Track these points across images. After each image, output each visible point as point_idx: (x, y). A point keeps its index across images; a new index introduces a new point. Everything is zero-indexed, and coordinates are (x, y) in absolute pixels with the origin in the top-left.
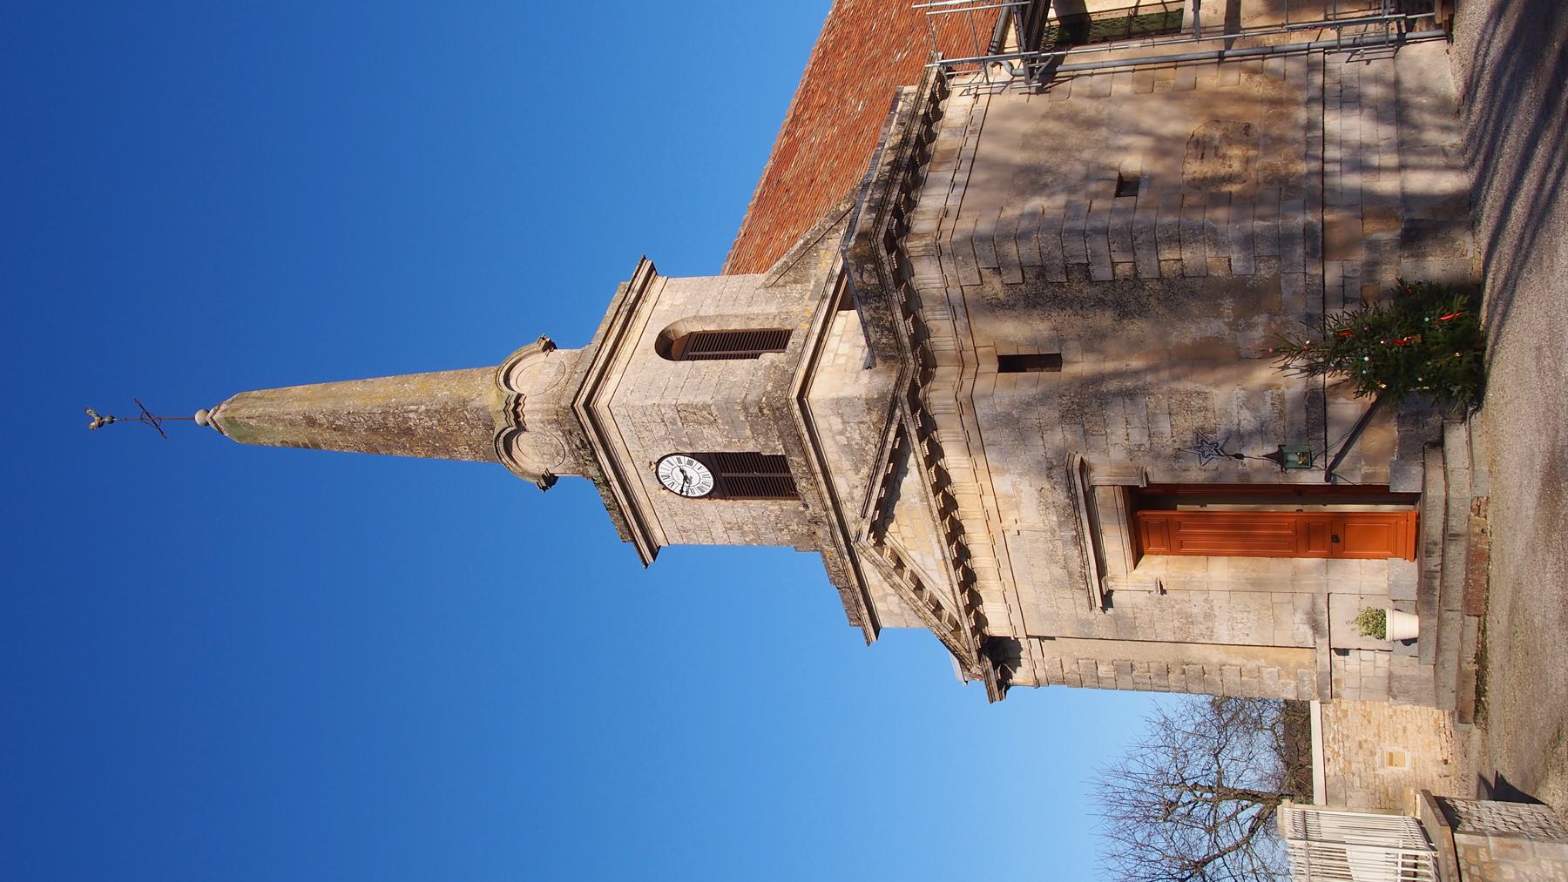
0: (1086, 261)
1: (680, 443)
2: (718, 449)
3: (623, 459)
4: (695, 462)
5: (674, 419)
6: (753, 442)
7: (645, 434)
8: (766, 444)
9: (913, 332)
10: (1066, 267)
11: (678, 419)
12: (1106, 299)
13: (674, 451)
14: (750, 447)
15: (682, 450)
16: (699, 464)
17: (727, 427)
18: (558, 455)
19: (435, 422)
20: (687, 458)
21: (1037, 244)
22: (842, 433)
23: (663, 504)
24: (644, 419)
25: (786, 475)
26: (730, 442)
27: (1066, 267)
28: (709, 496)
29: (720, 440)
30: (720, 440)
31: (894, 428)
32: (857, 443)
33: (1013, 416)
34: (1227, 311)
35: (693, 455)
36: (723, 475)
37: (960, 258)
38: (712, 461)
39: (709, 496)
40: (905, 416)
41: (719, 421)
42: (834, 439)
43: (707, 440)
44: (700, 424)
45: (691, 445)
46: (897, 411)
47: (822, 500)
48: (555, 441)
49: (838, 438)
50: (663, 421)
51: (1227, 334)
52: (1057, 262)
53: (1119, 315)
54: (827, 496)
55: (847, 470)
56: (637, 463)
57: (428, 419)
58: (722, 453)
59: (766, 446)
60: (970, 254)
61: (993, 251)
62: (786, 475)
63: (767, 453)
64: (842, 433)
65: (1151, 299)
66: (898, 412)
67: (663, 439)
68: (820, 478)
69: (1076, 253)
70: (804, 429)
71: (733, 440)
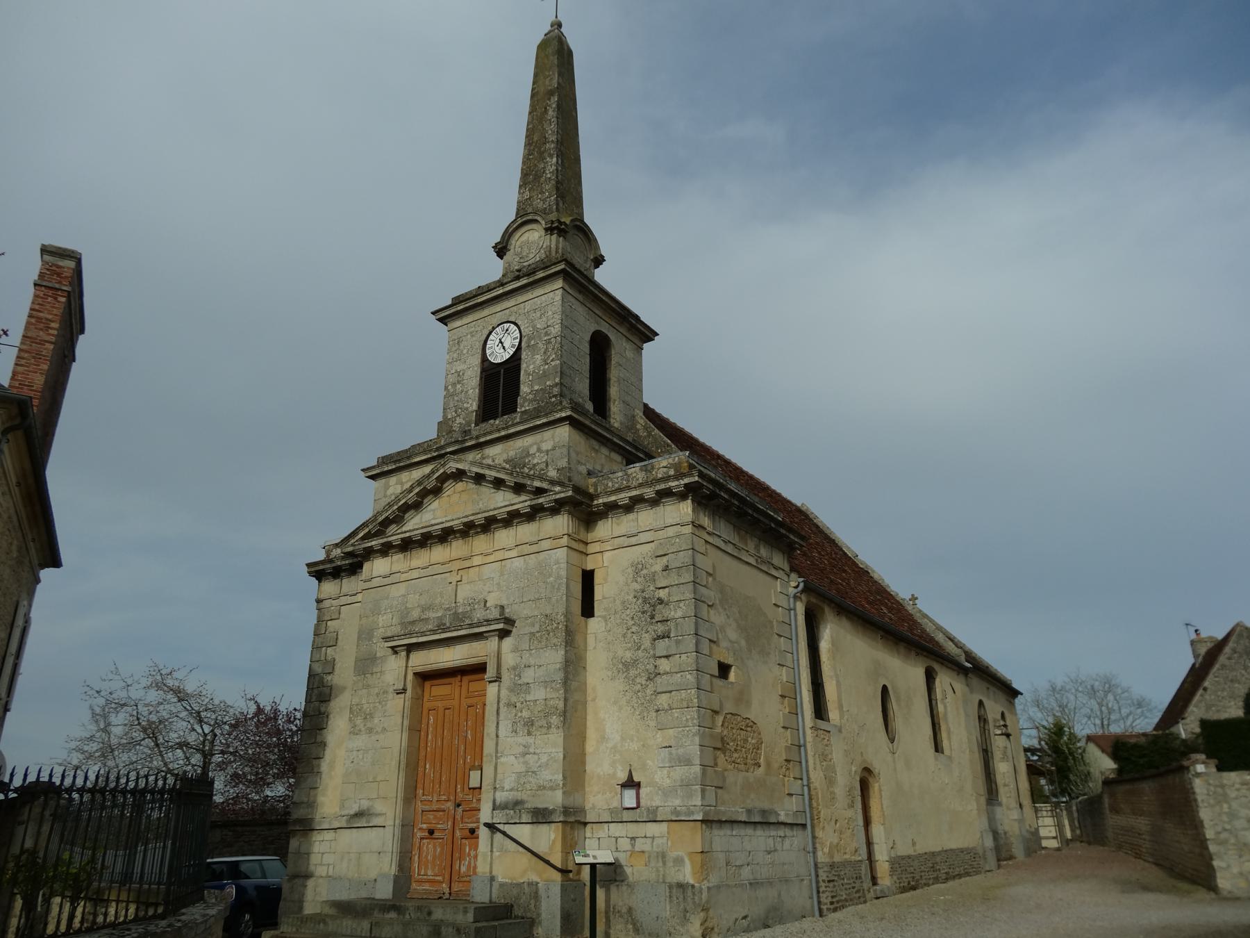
0: (672, 635)
1: (530, 339)
2: (523, 366)
3: (521, 299)
4: (514, 350)
5: (548, 335)
6: (529, 391)
7: (538, 314)
8: (527, 400)
9: (619, 503)
10: (667, 621)
11: (549, 337)
12: (640, 651)
13: (523, 334)
14: (524, 389)
15: (524, 340)
16: (512, 353)
17: (541, 372)
18: (521, 258)
19: (549, 176)
20: (517, 344)
21: (688, 598)
22: (539, 450)
23: (481, 327)
24: (550, 313)
25: (500, 414)
26: (529, 374)
27: (667, 621)
28: (484, 359)
29: (532, 367)
30: (532, 367)
31: (545, 485)
32: (530, 461)
33: (549, 578)
34: (627, 744)
35: (519, 348)
36: (502, 371)
37: (677, 540)
38: (514, 363)
39: (484, 359)
40: (555, 494)
41: (547, 367)
42: (535, 443)
43: (532, 358)
44: (545, 353)
45: (528, 346)
46: (560, 488)
47: (485, 435)
48: (531, 256)
49: (535, 447)
50: (548, 326)
51: (607, 745)
52: (672, 613)
53: (626, 661)
54: (488, 438)
55: (507, 453)
56: (515, 308)
57: (551, 171)
58: (520, 369)
59: (525, 400)
60: (681, 548)
61: (683, 565)
62: (500, 414)
63: (520, 400)
64: (539, 450)
65: (639, 685)
66: (558, 489)
67: (534, 327)
68: (503, 433)
69: (679, 628)
70: (544, 420)
71: (531, 377)
